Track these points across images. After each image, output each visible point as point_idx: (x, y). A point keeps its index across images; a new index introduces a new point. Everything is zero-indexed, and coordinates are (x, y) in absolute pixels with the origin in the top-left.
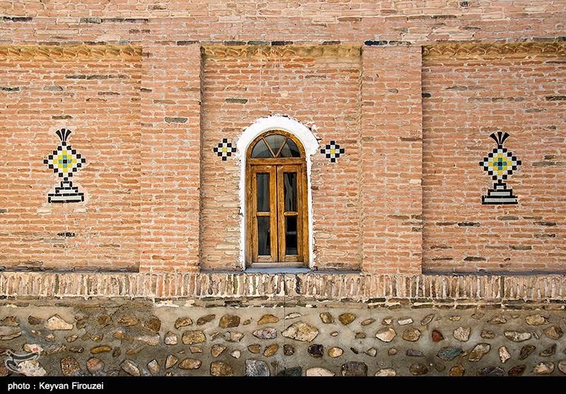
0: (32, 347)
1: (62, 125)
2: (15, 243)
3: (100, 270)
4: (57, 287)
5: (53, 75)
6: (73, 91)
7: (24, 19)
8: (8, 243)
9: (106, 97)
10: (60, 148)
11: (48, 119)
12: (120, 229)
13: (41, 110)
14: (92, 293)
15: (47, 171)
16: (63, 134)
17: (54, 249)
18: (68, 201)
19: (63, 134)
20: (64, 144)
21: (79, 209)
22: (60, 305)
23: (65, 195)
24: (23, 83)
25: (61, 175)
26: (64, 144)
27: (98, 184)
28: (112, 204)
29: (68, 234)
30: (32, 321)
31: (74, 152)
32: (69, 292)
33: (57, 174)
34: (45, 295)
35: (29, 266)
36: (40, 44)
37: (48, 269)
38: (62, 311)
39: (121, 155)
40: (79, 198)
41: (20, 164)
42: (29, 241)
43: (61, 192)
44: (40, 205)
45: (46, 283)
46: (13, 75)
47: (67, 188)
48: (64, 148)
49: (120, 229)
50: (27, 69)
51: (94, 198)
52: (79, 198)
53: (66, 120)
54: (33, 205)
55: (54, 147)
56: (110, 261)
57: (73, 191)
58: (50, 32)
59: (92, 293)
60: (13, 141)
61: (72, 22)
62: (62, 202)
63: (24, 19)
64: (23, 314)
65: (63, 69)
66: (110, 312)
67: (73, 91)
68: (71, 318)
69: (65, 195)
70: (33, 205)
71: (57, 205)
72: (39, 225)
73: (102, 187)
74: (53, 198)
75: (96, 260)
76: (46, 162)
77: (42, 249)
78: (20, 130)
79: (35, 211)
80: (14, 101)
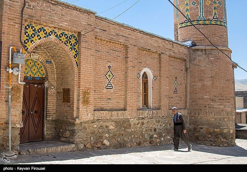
0: (107, 135)
1: (109, 64)
2: (98, 101)
3: (119, 110)
4: (111, 116)
5: (107, 48)
6: (111, 54)
7: (105, 31)
8: (96, 101)
9: (118, 57)
10: (109, 72)
11: (106, 62)
12: (120, 97)
13: (105, 59)
14: (118, 117)
15: (106, 78)
16: (109, 67)
17: (106, 103)
18: (110, 88)
19: (109, 67)
20: (109, 70)
21: (112, 91)
22: (112, 121)
23: (109, 86)
24: (100, 49)
25: (108, 80)
26: (109, 70)
27: (116, 84)
28: (119, 90)
29: (109, 99)
30: (107, 127)
31: (111, 73)
32: (114, 117)
33: (108, 80)
34: (109, 118)
35: (101, 109)
36: (108, 39)
37: (105, 110)
38: (113, 123)
39: (121, 75)
40: (112, 87)
41: (100, 76)
42: (101, 101)
43: (109, 85)
44: (103, 89)
45: (109, 115)
46: (99, 46)
47: (110, 84)
48: (109, 71)
49: (120, 97)
50: (102, 45)
51: (115, 88)
52: (112, 87)
53: (110, 63)
54: (103, 89)
55: (107, 71)
56: (118, 107)
57: (111, 85)
58: (110, 36)
59: (118, 117)
60: (98, 68)
61: (114, 34)
62: (108, 88)
63: (105, 31)
64: (104, 124)
65: (109, 47)
66: (122, 123)
67: (111, 54)
68: (114, 125)
69: (109, 86)
70: (103, 89)
71: (107, 89)
72: (103, 96)
73: (117, 84)
74: (107, 87)
75: (115, 107)
76: (106, 75)
77: (104, 103)
78: (100, 65)
79: (103, 91)
80: (99, 55)
